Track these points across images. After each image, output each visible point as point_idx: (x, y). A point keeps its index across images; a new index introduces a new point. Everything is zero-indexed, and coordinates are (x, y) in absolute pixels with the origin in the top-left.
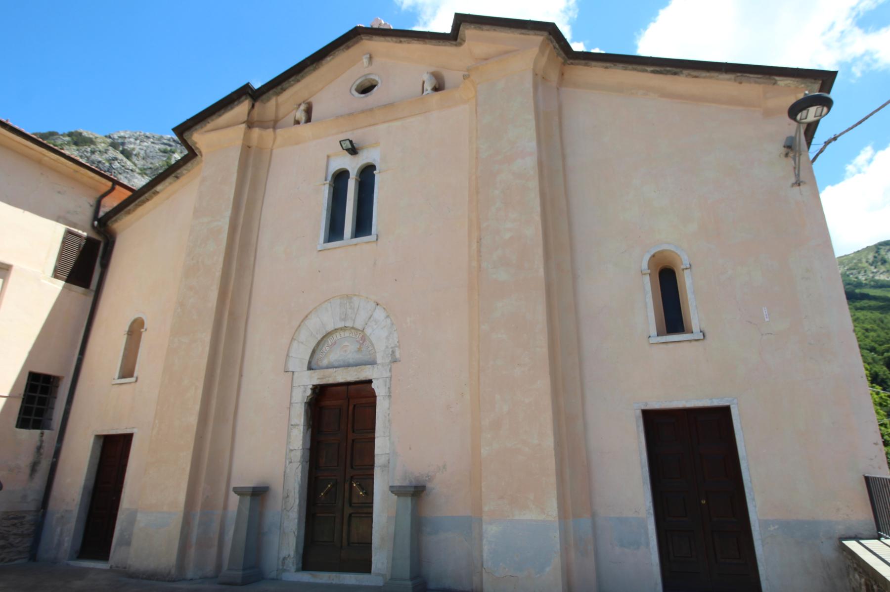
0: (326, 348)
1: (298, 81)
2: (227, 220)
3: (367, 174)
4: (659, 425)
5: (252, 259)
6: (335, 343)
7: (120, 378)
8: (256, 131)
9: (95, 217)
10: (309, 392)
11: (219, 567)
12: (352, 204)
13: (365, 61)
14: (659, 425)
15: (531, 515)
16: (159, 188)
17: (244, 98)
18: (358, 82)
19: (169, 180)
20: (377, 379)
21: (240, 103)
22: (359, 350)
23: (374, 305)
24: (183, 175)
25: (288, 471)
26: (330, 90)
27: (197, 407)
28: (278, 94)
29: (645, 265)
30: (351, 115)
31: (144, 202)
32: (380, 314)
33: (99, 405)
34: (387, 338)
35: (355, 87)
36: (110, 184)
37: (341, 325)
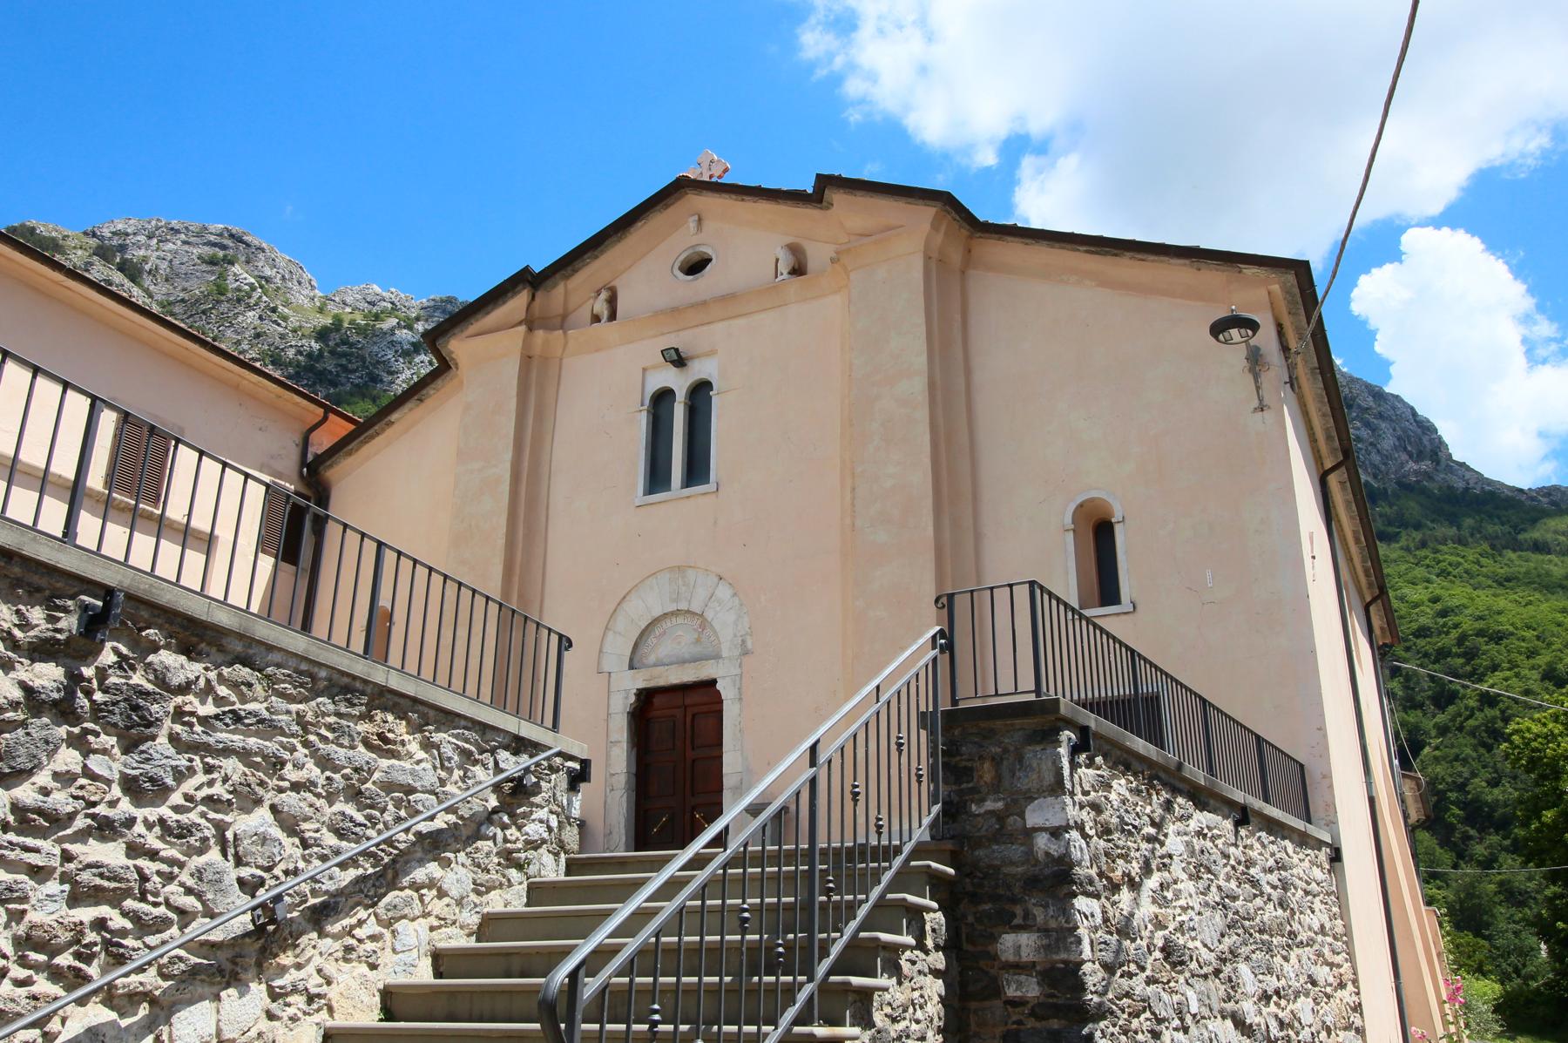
0: (652, 640)
1: (597, 257)
2: (508, 465)
3: (701, 391)
5: (543, 519)
9: (303, 462)
10: (632, 699)
13: (692, 224)
16: (394, 417)
18: (682, 258)
19: (409, 405)
21: (515, 294)
22: (698, 641)
23: (716, 579)
26: (644, 276)
28: (567, 277)
30: (675, 311)
31: (372, 437)
32: (724, 592)
35: (677, 265)
36: (320, 411)
37: (673, 607)
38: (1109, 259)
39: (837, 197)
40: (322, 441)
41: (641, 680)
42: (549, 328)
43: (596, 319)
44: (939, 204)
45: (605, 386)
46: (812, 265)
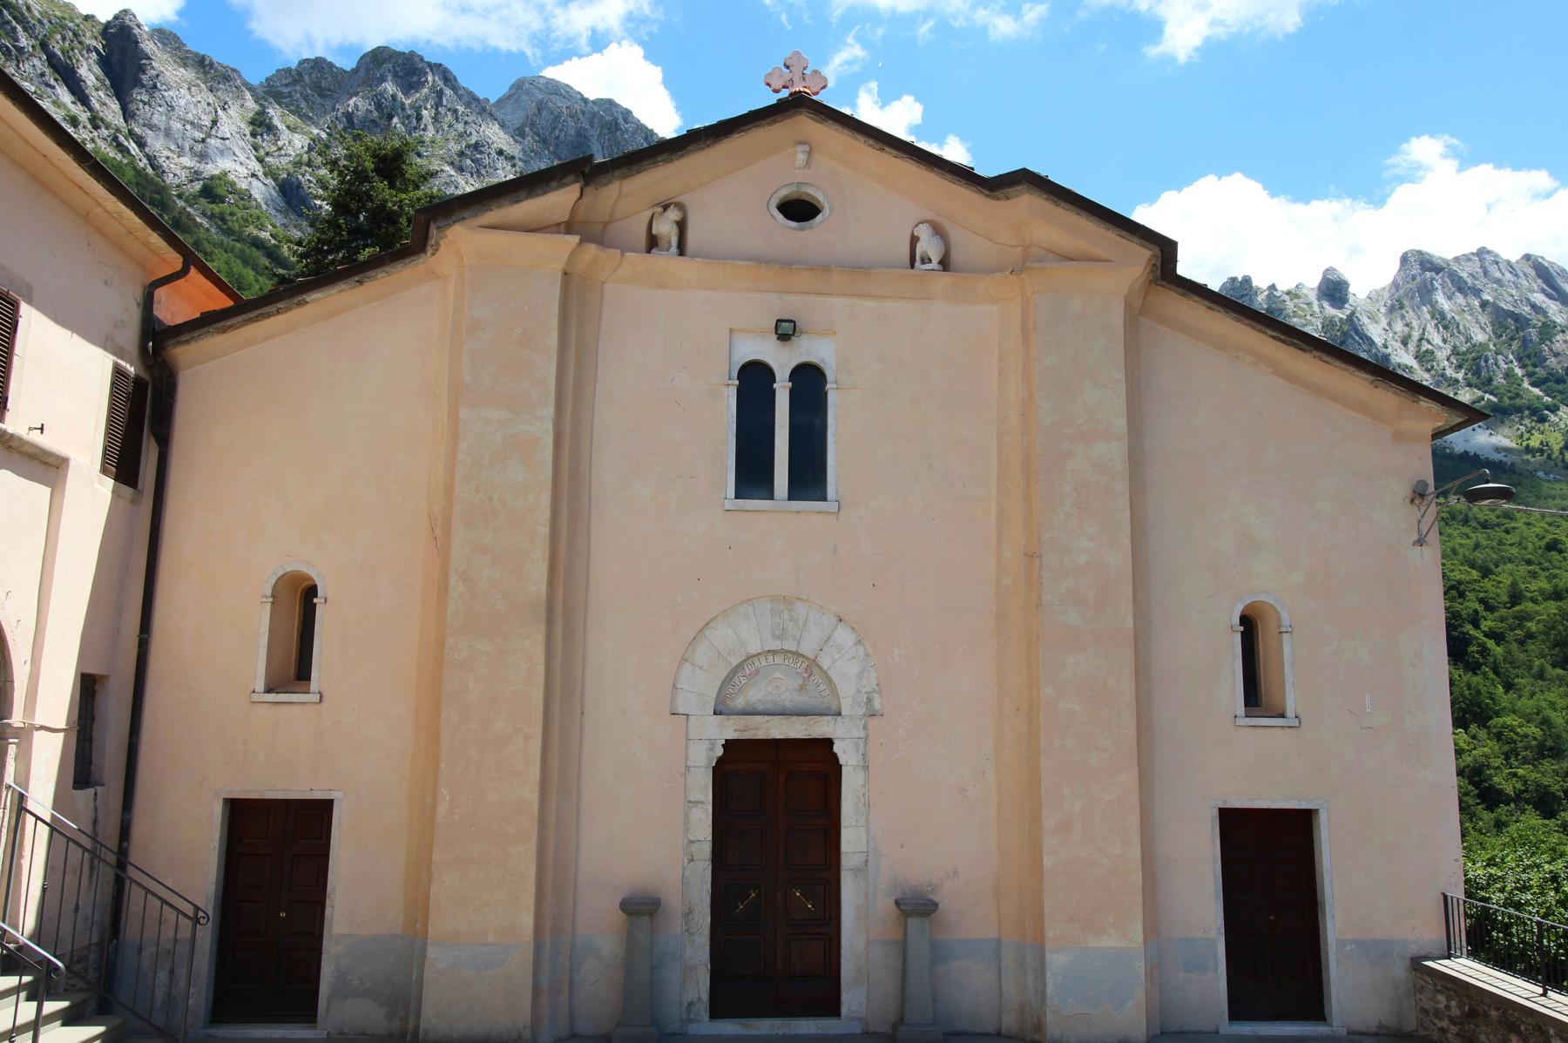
0: (740, 680)
2: (549, 425)
3: (809, 379)
6: (757, 672)
7: (269, 690)
8: (592, 248)
10: (720, 752)
12: (780, 434)
13: (801, 158)
17: (571, 178)
20: (843, 739)
22: (802, 688)
23: (835, 620)
24: (375, 278)
25: (687, 873)
27: (535, 771)
28: (625, 177)
32: (844, 636)
34: (859, 676)
35: (775, 202)
36: (175, 261)
37: (776, 645)
39: (1026, 202)
40: (173, 308)
41: (732, 729)
42: (602, 241)
43: (653, 243)
44: (1157, 250)
45: (680, 341)
46: (957, 257)
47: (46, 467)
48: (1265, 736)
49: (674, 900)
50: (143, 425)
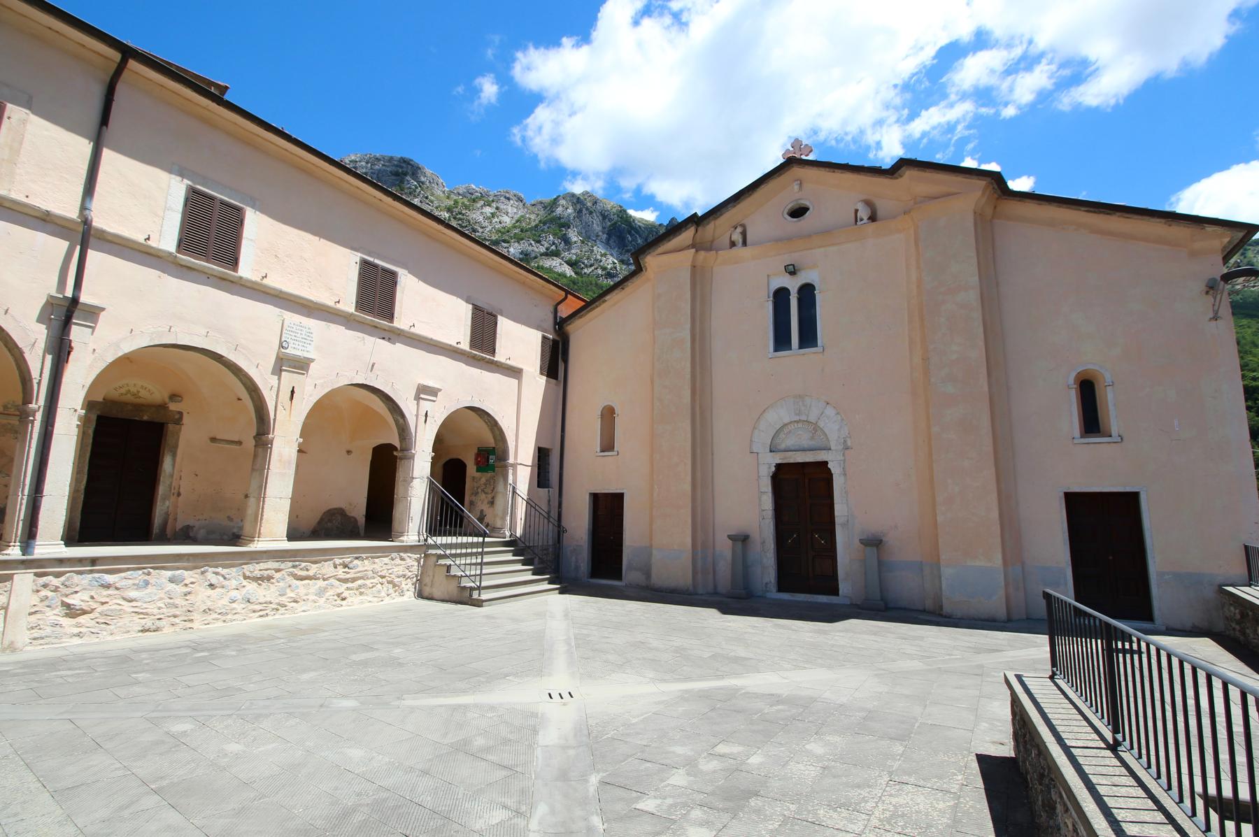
0: (782, 436)
3: (807, 292)
4: (1077, 504)
8: (702, 254)
9: (555, 323)
10: (773, 469)
11: (715, 587)
12: (795, 318)
13: (796, 187)
14: (1077, 504)
15: (981, 563)
16: (607, 298)
22: (812, 438)
27: (689, 478)
29: (1071, 380)
30: (789, 239)
32: (830, 411)
33: (588, 473)
37: (797, 418)
38: (1101, 216)
40: (564, 312)
41: (778, 459)
43: (733, 244)
44: (989, 179)
46: (880, 213)
47: (515, 372)
48: (1096, 447)
49: (755, 536)
50: (556, 359)
